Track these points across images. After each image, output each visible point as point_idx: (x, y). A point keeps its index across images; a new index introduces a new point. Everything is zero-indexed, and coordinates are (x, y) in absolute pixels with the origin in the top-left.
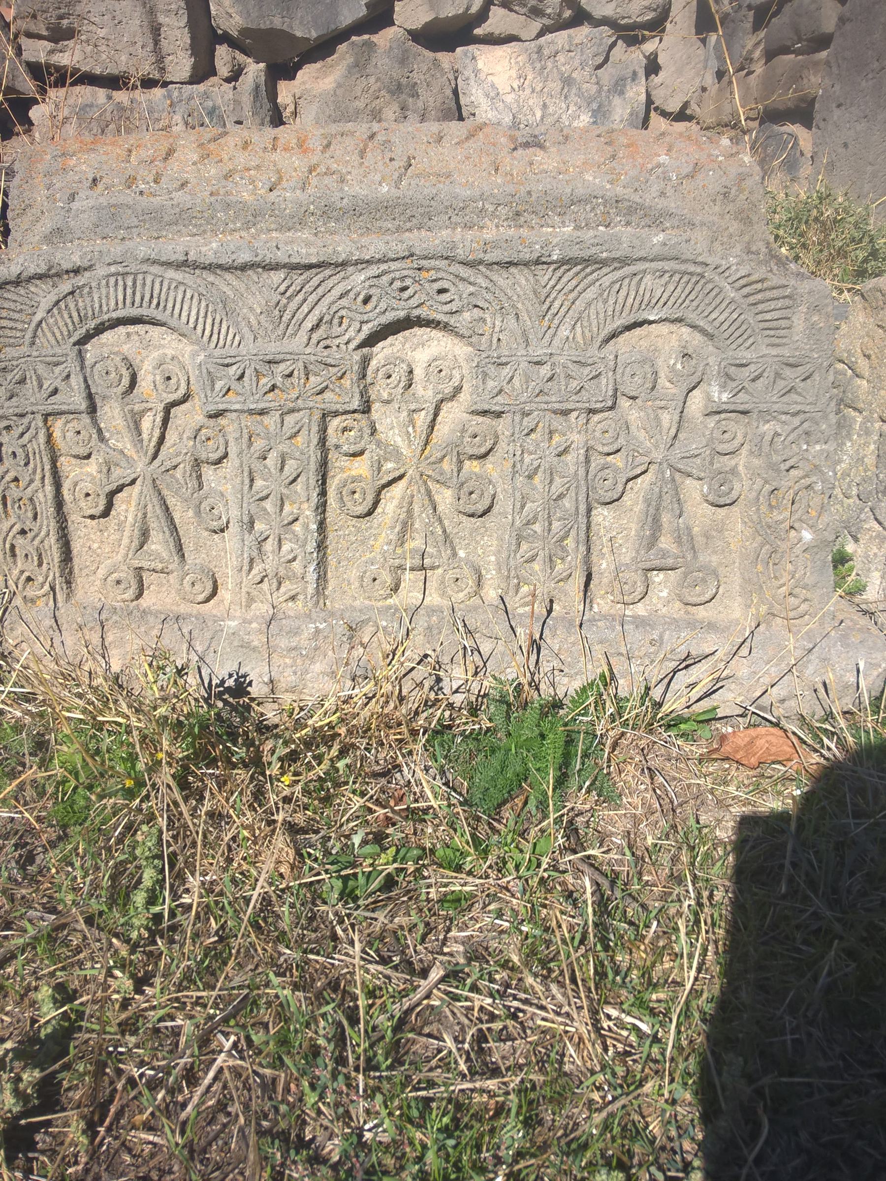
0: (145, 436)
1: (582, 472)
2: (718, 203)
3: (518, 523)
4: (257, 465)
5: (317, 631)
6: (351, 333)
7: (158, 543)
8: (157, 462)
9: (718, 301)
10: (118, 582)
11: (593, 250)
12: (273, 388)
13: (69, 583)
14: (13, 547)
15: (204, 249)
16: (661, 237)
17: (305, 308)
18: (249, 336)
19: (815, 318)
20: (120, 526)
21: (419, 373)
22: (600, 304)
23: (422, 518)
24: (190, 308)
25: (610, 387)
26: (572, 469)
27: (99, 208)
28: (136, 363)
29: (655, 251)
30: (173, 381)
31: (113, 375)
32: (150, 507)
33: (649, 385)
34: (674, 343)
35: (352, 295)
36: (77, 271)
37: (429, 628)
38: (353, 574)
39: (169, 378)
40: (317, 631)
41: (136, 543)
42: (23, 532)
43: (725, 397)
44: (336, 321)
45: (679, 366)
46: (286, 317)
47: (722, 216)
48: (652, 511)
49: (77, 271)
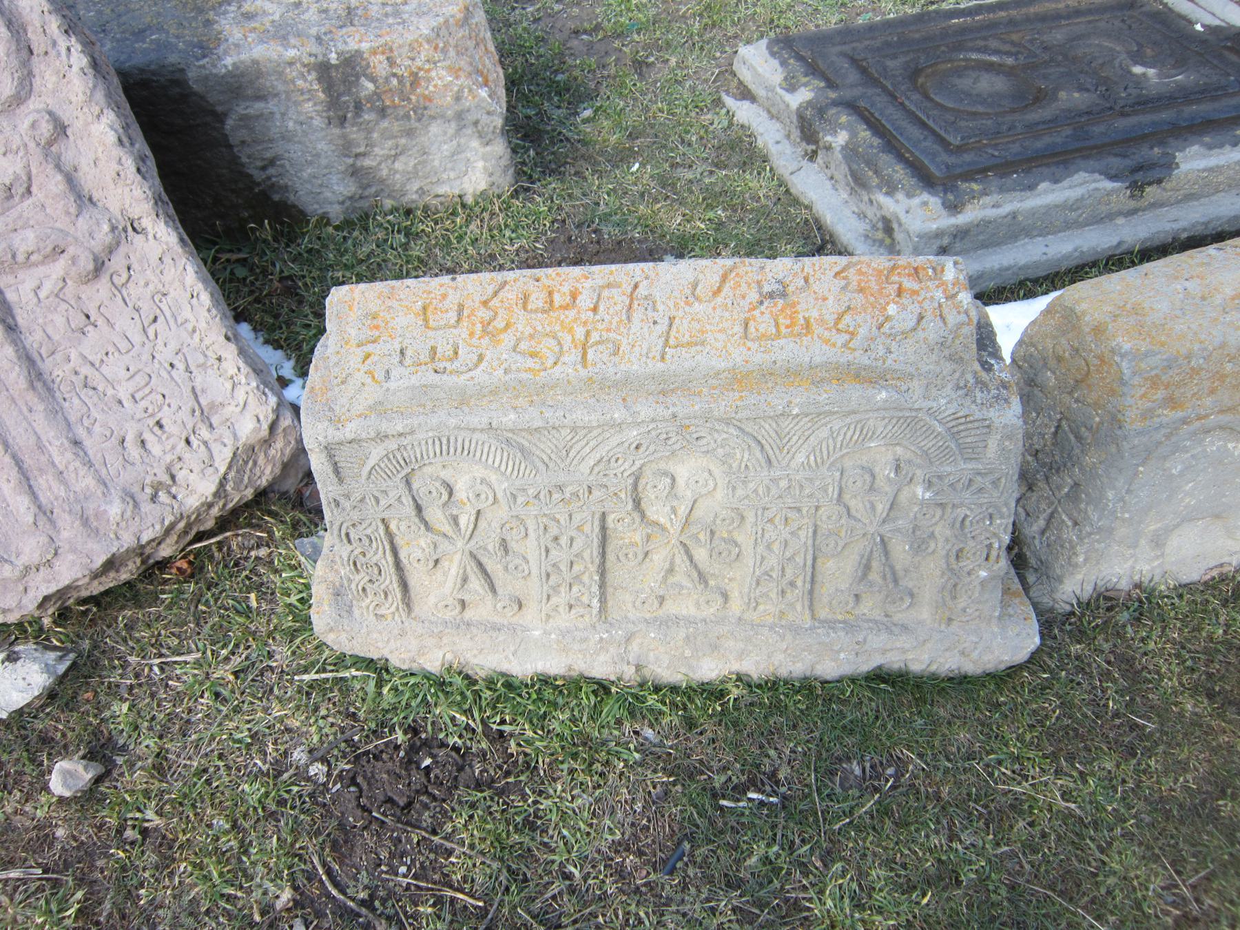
1: (810, 542)
2: (936, 351)
3: (757, 573)
5: (601, 639)
6: (626, 465)
7: (476, 583)
8: (472, 542)
13: (408, 605)
14: (364, 589)
15: (504, 420)
16: (884, 395)
17: (587, 449)
18: (542, 467)
19: (1007, 443)
20: (445, 574)
22: (831, 441)
25: (836, 492)
26: (803, 540)
27: (413, 388)
30: (483, 496)
32: (468, 568)
34: (890, 457)
36: (400, 435)
37: (688, 637)
40: (601, 639)
41: (458, 586)
43: (927, 495)
44: (613, 460)
45: (892, 475)
47: (937, 363)
48: (864, 561)
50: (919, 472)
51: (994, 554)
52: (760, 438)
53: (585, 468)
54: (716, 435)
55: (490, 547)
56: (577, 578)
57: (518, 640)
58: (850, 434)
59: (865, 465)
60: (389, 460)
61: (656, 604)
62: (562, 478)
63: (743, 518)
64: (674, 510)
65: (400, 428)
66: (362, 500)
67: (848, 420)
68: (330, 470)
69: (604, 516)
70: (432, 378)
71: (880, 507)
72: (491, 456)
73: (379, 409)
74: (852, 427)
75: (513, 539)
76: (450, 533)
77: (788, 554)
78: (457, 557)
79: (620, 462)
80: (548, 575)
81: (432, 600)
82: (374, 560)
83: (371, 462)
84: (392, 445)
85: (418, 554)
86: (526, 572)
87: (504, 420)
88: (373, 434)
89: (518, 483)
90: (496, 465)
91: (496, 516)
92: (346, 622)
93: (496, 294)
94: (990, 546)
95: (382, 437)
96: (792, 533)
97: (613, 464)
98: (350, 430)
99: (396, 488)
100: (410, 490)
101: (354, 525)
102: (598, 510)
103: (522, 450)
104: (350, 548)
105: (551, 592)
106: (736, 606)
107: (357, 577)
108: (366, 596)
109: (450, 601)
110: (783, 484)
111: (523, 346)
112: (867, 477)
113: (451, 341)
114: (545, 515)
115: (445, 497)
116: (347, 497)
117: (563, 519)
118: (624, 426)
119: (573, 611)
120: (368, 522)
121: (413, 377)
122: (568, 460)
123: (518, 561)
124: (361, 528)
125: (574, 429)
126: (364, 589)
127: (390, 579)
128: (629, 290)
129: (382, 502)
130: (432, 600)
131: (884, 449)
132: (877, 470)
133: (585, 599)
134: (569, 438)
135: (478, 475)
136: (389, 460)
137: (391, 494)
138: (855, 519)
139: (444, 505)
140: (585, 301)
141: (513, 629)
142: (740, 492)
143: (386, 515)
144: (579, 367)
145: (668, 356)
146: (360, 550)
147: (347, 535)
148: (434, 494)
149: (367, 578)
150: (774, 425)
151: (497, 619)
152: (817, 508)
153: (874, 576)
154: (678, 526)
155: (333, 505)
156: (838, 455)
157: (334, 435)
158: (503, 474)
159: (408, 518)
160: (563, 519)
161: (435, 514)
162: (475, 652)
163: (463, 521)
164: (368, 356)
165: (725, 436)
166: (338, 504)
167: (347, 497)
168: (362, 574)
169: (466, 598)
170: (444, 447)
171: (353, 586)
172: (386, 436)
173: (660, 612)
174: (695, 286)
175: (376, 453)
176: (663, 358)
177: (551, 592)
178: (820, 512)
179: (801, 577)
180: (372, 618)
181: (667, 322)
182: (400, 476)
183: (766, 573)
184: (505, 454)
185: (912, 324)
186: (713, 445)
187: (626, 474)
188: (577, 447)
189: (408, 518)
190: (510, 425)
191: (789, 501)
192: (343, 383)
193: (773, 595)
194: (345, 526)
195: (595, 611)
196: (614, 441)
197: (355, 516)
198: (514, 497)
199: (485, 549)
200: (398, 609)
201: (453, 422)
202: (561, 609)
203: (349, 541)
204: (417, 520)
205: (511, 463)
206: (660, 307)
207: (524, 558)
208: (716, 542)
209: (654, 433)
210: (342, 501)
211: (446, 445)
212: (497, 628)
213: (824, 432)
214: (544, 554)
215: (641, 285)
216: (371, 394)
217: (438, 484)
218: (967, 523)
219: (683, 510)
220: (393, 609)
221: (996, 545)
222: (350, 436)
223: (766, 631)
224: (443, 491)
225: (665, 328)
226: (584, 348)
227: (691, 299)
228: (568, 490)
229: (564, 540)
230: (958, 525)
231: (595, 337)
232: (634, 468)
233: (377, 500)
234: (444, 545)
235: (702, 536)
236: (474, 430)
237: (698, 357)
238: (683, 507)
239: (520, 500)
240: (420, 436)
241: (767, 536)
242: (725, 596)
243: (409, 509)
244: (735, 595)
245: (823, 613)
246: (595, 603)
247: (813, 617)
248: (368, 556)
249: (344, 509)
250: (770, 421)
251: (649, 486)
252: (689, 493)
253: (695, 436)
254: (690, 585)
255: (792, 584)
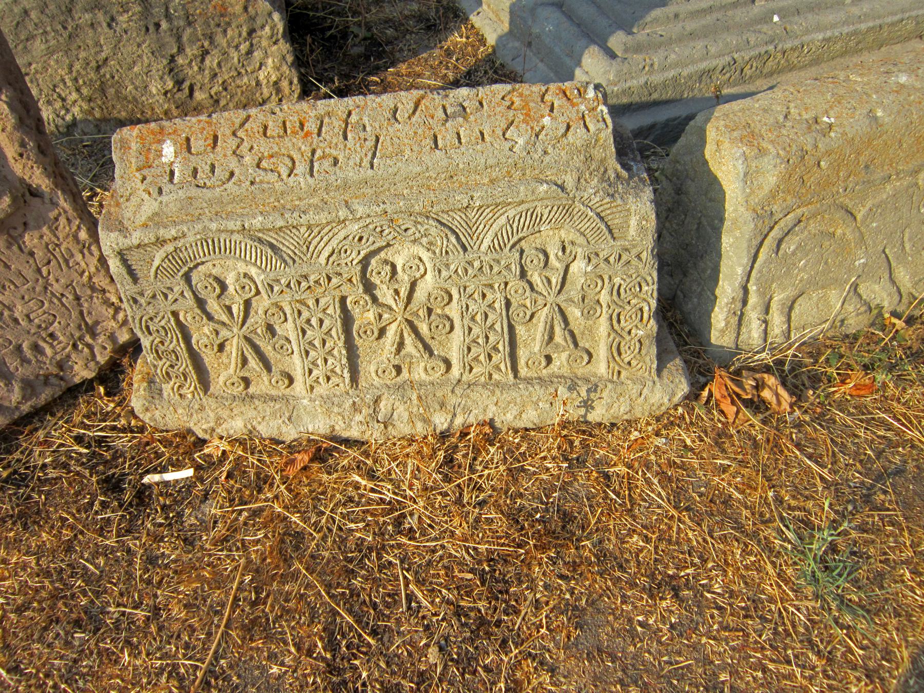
0: (235, 315)
1: (504, 313)
3: (467, 341)
4: (306, 326)
6: (354, 255)
7: (253, 363)
8: (245, 328)
9: (582, 217)
10: (233, 384)
11: (501, 199)
12: (309, 287)
14: (167, 373)
15: (254, 222)
21: (399, 269)
22: (508, 227)
23: (409, 340)
24: (251, 253)
25: (518, 270)
26: (499, 311)
28: (222, 278)
29: (541, 196)
30: (247, 288)
31: (209, 288)
32: (245, 349)
33: (542, 265)
35: (351, 238)
36: (175, 239)
38: (372, 368)
39: (244, 287)
41: (240, 365)
42: (172, 366)
45: (560, 253)
46: (311, 249)
49: (175, 239)
50: (579, 250)
51: (646, 316)
52: (454, 227)
53: (322, 259)
54: (419, 226)
55: (259, 331)
56: (330, 353)
57: (291, 408)
58: (522, 220)
59: (539, 246)
60: (169, 260)
61: (394, 373)
62: (305, 270)
63: (450, 296)
64: (397, 292)
65: (173, 232)
66: (154, 297)
67: (519, 209)
68: (124, 271)
69: (343, 300)
70: (194, 192)
71: (554, 281)
72: (248, 253)
73: (156, 220)
74: (524, 214)
75: (276, 322)
76: (228, 322)
77: (489, 323)
78: (235, 340)
79: (348, 253)
80: (307, 353)
81: (221, 380)
82: (171, 347)
83: (156, 263)
84: (170, 248)
85: (205, 340)
86: (290, 351)
87: (254, 222)
88: (153, 240)
89: (272, 275)
90: (253, 260)
91: (262, 304)
92: (157, 402)
93: (242, 125)
94: (641, 309)
95: (160, 242)
96: (489, 306)
97: (343, 254)
98: (135, 238)
99: (179, 286)
100: (190, 286)
101: (151, 319)
102: (338, 294)
103: (272, 246)
104: (151, 338)
105: (311, 366)
106: (456, 371)
107: (161, 363)
108: (171, 379)
109: (235, 379)
110: (477, 264)
111: (264, 164)
112: (541, 256)
113: (209, 162)
114: (297, 301)
115: (218, 291)
116: (142, 294)
117: (311, 302)
118: (347, 223)
119: (331, 382)
120: (161, 314)
121: (180, 192)
122: (309, 254)
123: (282, 342)
124: (156, 320)
125: (309, 227)
126: (167, 373)
127: (185, 364)
128: (345, 116)
129: (170, 297)
130: (221, 380)
131: (551, 233)
132: (548, 250)
133: (338, 370)
134: (306, 235)
135: (242, 271)
136: (169, 260)
137: (175, 289)
138: (537, 292)
139: (219, 297)
140: (311, 126)
141: (285, 399)
142: (444, 273)
143: (174, 307)
144: (308, 176)
145: (375, 165)
146: (158, 340)
147: (148, 327)
148: (209, 288)
149: (168, 363)
150: (464, 216)
151: (274, 392)
152: (506, 284)
153: (559, 338)
154: (401, 305)
155: (131, 302)
156: (515, 239)
157: (124, 243)
158: (260, 268)
159: (192, 309)
160: (311, 302)
161: (213, 306)
162: (260, 419)
163: (235, 310)
164: (144, 179)
165: (426, 227)
166: (135, 301)
167: (142, 294)
168: (164, 360)
169: (247, 375)
170: (211, 247)
171: (159, 371)
172: (165, 241)
173: (398, 379)
174: (396, 110)
175: (159, 256)
176: (372, 167)
177: (311, 366)
178: (508, 287)
179: (501, 343)
180: (177, 397)
181: (374, 138)
182: (180, 274)
183: (474, 341)
184: (259, 251)
185: (563, 130)
186: (418, 235)
187: (354, 263)
188: (314, 243)
189: (192, 309)
190: (259, 226)
191: (484, 280)
192: (127, 200)
193: (482, 358)
194: (144, 319)
195: (347, 380)
196: (342, 235)
197: (151, 311)
198: (272, 288)
199: (256, 333)
200: (196, 388)
201: (214, 226)
202: (321, 380)
203: (150, 334)
204: (199, 312)
205: (264, 258)
206: (368, 129)
207: (288, 340)
208: (433, 317)
209: (371, 227)
210: (138, 298)
211: (212, 245)
212: (273, 399)
213: (503, 220)
214: (300, 334)
215: (353, 112)
216: (150, 206)
217: (211, 280)
218: (622, 290)
219: (403, 293)
220: (192, 388)
221: (646, 309)
222: (136, 242)
223: (480, 388)
224: (215, 285)
225: (373, 143)
226: (312, 162)
227: (393, 121)
228: (312, 278)
229: (314, 321)
230: (615, 293)
231: (319, 153)
232: (360, 257)
233: (166, 296)
234: (224, 333)
235: (421, 313)
236: (232, 232)
237: (399, 164)
238: (403, 289)
239: (276, 289)
240: (191, 238)
241: (470, 310)
242: (448, 364)
243: (190, 302)
244: (454, 362)
245: (523, 372)
246: (347, 375)
247: (516, 377)
248: (166, 344)
249: (141, 305)
250: (459, 213)
251: (374, 274)
252: (406, 278)
253: (403, 227)
254: (418, 355)
255: (495, 349)
